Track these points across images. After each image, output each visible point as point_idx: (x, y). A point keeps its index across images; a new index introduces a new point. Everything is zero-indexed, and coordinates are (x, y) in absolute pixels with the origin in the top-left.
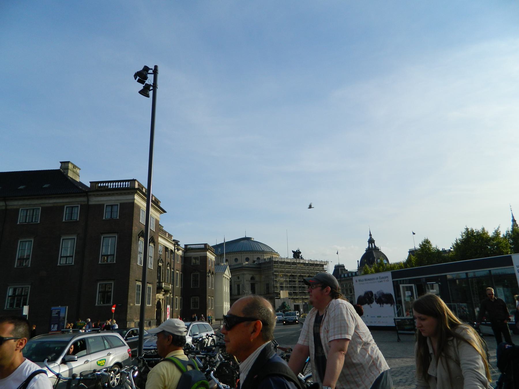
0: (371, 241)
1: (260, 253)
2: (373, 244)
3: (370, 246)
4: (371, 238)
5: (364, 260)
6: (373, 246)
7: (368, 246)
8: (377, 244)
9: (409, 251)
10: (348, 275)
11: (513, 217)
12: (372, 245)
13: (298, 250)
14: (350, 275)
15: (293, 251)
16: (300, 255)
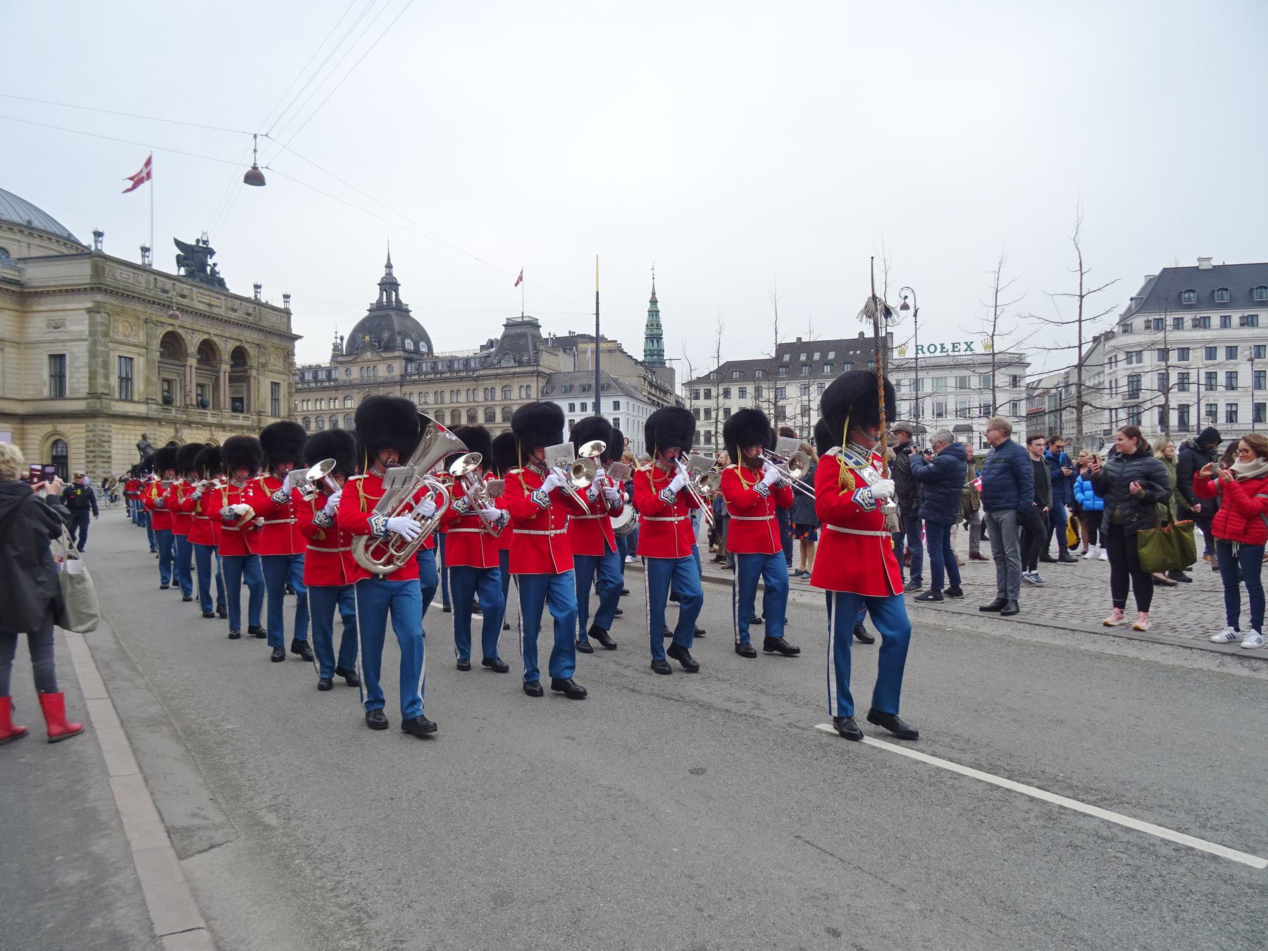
0: (389, 285)
1: (11, 229)
2: (394, 293)
3: (385, 300)
4: (389, 274)
5: (364, 338)
6: (394, 300)
7: (377, 297)
8: (405, 295)
9: (505, 323)
10: (302, 379)
11: (654, 294)
12: (389, 297)
13: (205, 242)
14: (309, 376)
15: (179, 244)
16: (210, 262)
